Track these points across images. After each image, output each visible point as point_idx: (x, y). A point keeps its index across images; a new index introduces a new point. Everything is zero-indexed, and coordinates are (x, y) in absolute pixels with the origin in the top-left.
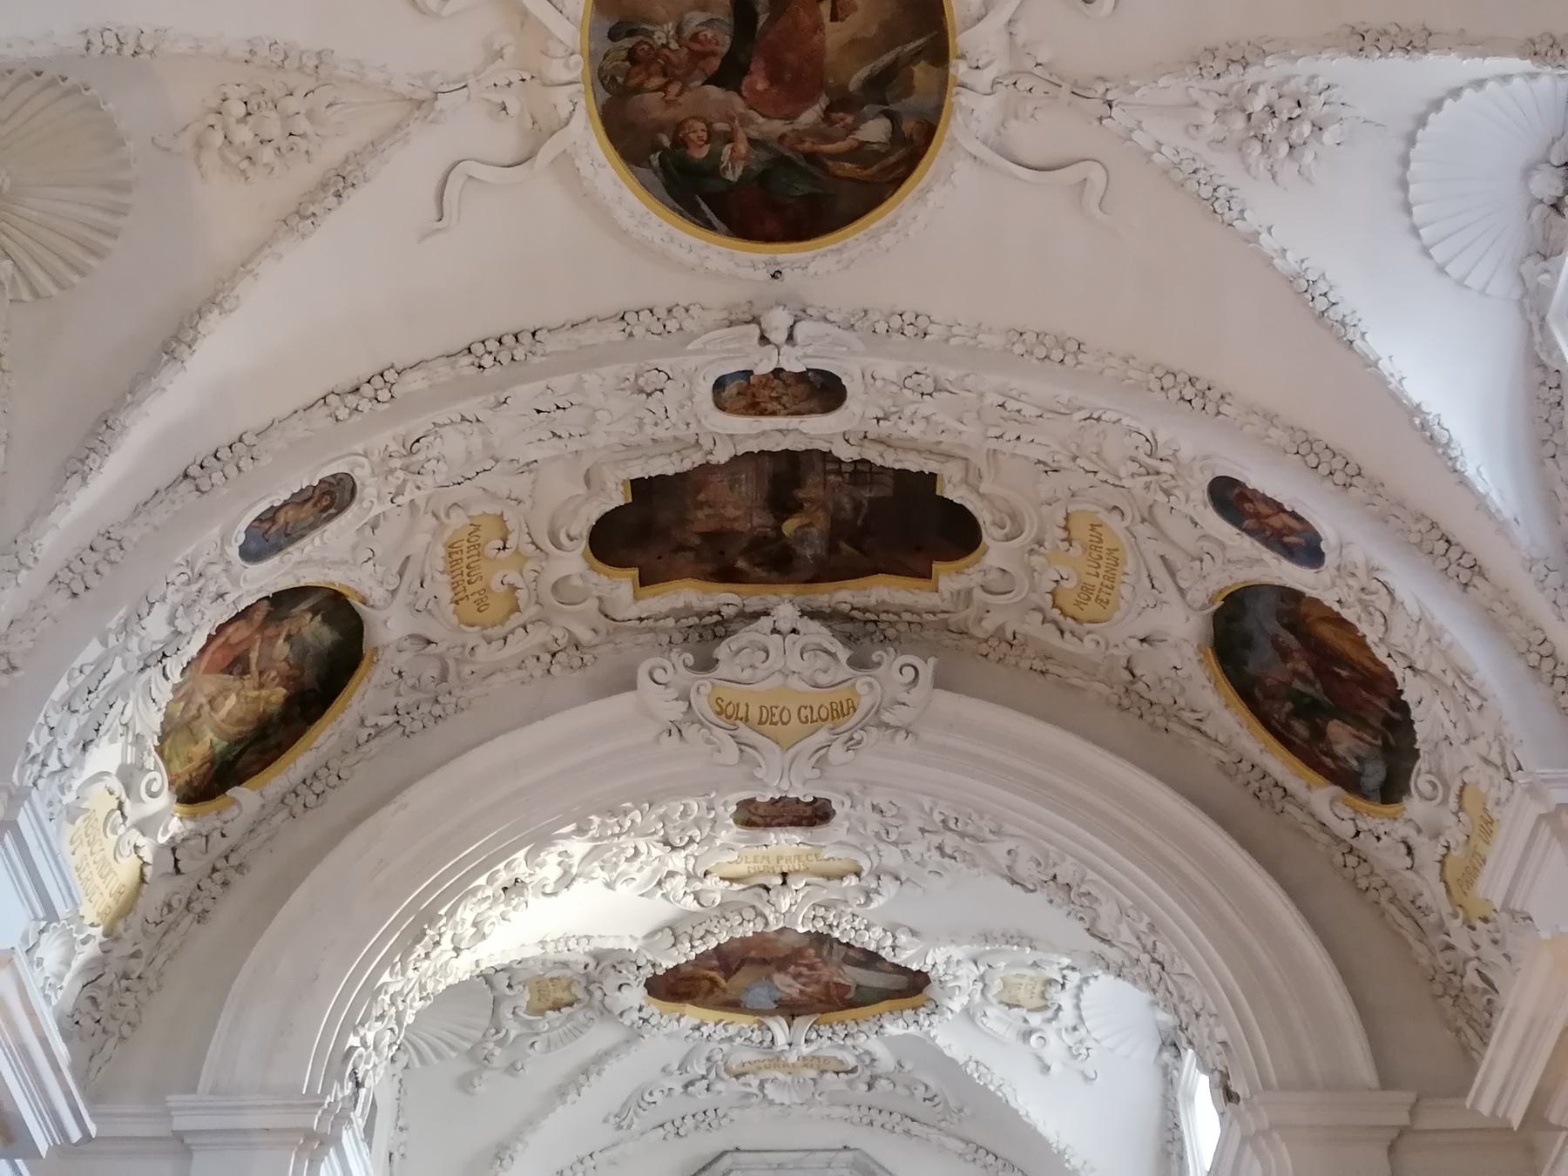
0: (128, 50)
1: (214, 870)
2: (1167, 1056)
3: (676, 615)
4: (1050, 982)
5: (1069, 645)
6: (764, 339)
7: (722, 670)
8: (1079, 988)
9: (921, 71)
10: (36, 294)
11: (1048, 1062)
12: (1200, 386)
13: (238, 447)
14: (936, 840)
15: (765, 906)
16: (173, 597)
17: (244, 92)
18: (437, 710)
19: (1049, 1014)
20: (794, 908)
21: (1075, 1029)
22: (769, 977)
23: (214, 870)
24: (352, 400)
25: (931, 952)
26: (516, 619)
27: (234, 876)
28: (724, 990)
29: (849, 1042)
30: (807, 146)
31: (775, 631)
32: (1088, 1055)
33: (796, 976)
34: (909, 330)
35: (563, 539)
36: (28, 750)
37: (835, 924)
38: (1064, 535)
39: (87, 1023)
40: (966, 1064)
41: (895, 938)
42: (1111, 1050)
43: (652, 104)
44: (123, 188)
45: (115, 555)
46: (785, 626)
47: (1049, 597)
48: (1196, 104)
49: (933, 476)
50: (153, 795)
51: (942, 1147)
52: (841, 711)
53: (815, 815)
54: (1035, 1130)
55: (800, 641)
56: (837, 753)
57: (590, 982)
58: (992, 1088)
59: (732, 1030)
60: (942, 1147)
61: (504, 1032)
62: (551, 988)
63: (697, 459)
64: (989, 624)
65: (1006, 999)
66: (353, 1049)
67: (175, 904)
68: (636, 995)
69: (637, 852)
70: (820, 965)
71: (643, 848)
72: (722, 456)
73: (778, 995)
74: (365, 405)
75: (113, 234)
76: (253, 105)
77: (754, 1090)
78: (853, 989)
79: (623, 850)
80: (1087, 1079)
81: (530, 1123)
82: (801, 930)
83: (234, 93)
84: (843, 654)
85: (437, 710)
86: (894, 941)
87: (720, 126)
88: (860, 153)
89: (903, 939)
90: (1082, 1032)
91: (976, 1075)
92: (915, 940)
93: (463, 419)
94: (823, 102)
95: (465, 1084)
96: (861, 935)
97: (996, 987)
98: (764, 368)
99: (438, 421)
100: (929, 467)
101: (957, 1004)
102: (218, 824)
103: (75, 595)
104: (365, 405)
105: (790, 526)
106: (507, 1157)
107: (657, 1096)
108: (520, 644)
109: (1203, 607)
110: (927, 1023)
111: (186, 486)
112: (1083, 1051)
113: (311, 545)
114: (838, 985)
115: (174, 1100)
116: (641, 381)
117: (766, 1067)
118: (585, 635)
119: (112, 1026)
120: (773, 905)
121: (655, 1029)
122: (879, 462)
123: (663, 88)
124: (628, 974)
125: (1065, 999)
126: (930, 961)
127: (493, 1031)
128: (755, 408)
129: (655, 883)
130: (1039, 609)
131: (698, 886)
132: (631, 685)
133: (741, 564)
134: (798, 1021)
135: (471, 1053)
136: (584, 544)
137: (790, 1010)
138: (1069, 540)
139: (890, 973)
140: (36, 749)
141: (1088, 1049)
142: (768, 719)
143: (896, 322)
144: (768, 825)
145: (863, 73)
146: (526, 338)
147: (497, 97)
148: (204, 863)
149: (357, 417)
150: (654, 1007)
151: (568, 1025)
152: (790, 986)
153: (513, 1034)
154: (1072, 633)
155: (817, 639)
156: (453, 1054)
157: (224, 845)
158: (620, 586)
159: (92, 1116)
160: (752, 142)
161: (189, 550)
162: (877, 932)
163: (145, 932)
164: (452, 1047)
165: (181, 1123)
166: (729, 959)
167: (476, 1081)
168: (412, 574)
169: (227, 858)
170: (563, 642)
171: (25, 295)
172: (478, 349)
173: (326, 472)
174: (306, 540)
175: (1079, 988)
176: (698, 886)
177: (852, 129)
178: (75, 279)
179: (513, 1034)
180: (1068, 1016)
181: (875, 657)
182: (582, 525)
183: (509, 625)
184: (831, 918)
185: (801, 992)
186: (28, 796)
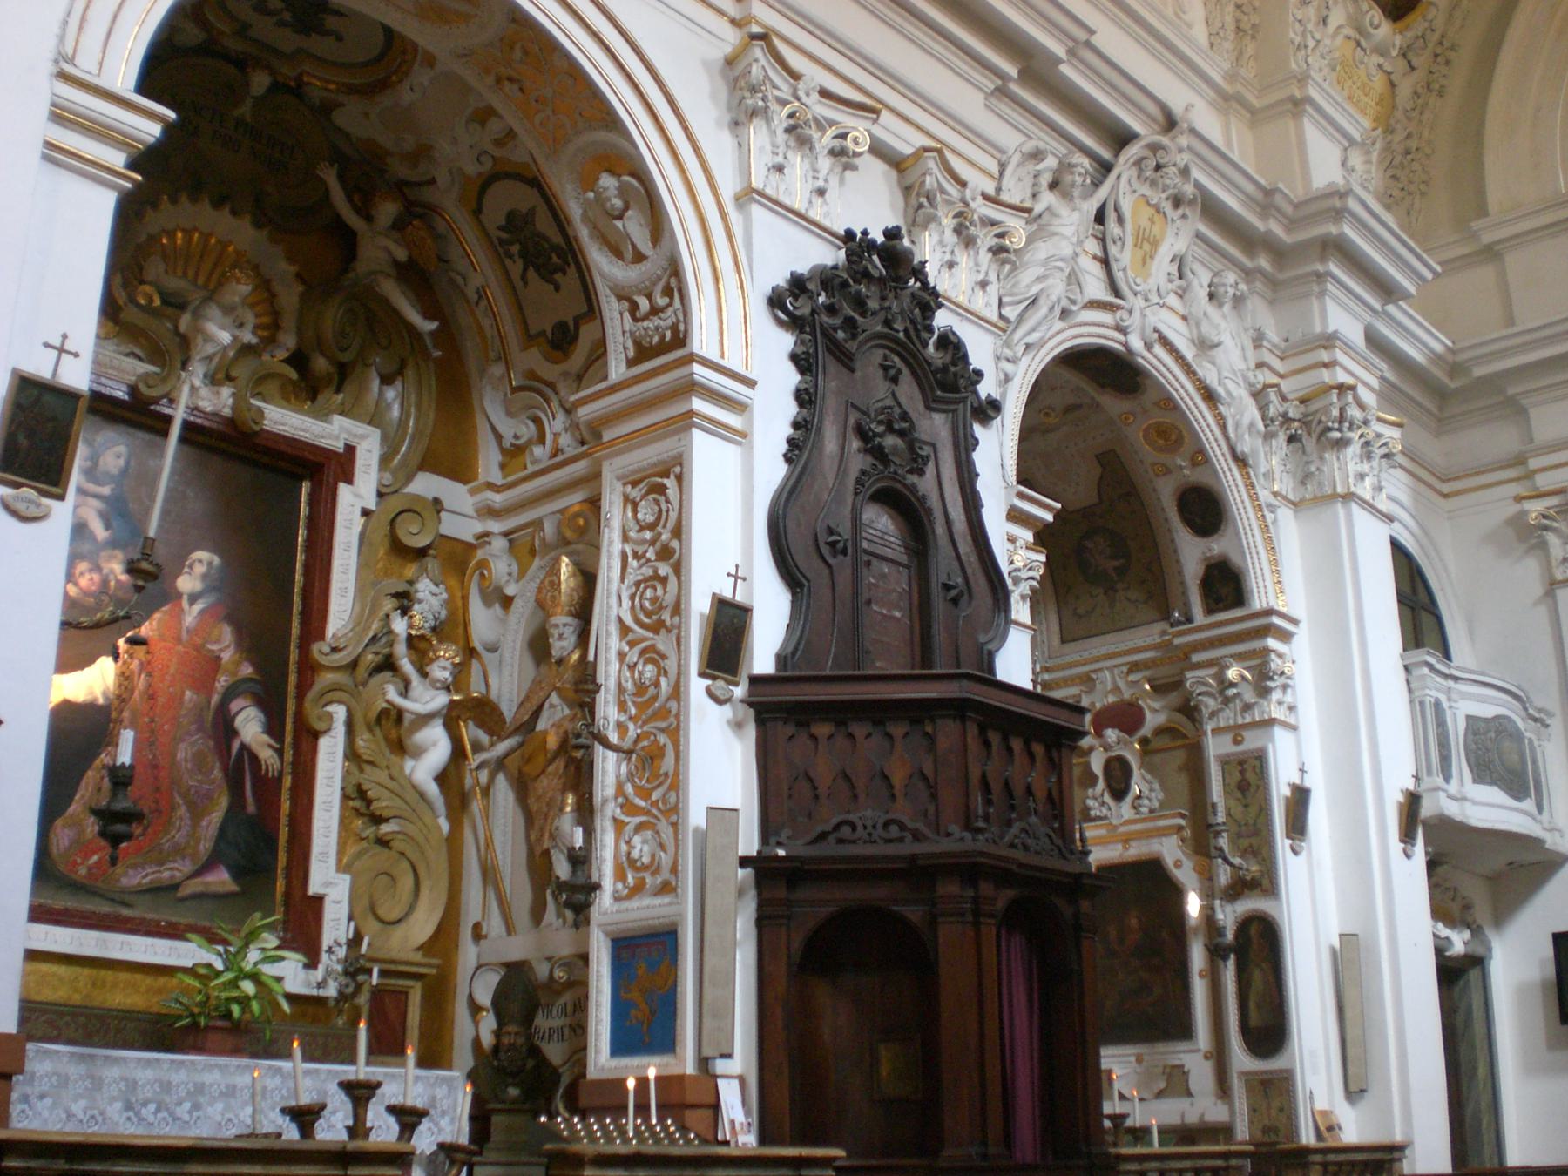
1: (1436, 56)
23: (1436, 56)
27: (1452, 55)
36: (1293, 42)
39: (1396, 193)
50: (1376, 27)
67: (1420, 90)
102: (1426, 24)
115: (1476, 225)
119: (1412, 188)
140: (1298, 40)
148: (1428, 53)
157: (1437, 36)
159: (1425, 251)
163: (1409, 119)
165: (1487, 238)
169: (1441, 43)
186: (1309, 77)
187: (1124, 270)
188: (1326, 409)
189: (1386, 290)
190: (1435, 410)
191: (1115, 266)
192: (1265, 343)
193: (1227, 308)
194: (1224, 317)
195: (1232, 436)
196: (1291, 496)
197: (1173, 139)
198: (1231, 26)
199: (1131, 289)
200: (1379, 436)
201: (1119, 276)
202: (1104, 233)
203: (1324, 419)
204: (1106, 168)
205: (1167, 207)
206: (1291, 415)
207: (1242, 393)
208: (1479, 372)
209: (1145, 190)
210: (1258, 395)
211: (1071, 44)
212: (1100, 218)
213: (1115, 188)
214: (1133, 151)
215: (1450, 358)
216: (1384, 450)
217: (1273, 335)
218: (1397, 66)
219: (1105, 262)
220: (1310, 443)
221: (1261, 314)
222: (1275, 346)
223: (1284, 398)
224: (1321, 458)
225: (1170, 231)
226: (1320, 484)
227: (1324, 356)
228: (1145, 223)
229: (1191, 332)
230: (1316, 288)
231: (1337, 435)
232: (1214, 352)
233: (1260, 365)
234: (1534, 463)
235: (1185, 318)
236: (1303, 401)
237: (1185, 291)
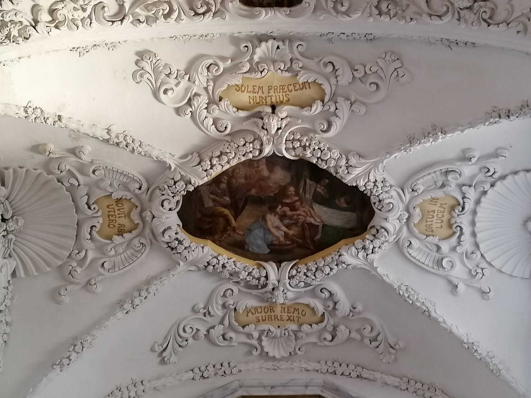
11: (455, 281)
15: (260, 131)
20: (280, 131)
22: (264, 218)
25: (372, 172)
28: (234, 229)
32: (483, 275)
37: (307, 144)
40: (399, 287)
41: (348, 160)
54: (451, 332)
58: (418, 304)
61: (83, 254)
62: (117, 212)
70: (298, 203)
73: (270, 238)
77: (255, 342)
78: (320, 229)
81: (98, 323)
86: (347, 163)
89: (353, 161)
91: (407, 295)
92: (363, 161)
96: (325, 154)
106: (79, 343)
110: (371, 247)
112: (479, 271)
114: (311, 225)
117: (264, 321)
120: (266, 130)
121: (187, 251)
127: (77, 252)
129: (186, 101)
134: (283, 265)
135: (60, 268)
139: (345, 210)
141: (482, 269)
144: (262, 5)
151: (128, 252)
152: (278, 228)
156: (48, 269)
162: (336, 154)
164: (48, 264)
167: (63, 292)
179: (91, 255)
184: (305, 140)
185: (286, 235)
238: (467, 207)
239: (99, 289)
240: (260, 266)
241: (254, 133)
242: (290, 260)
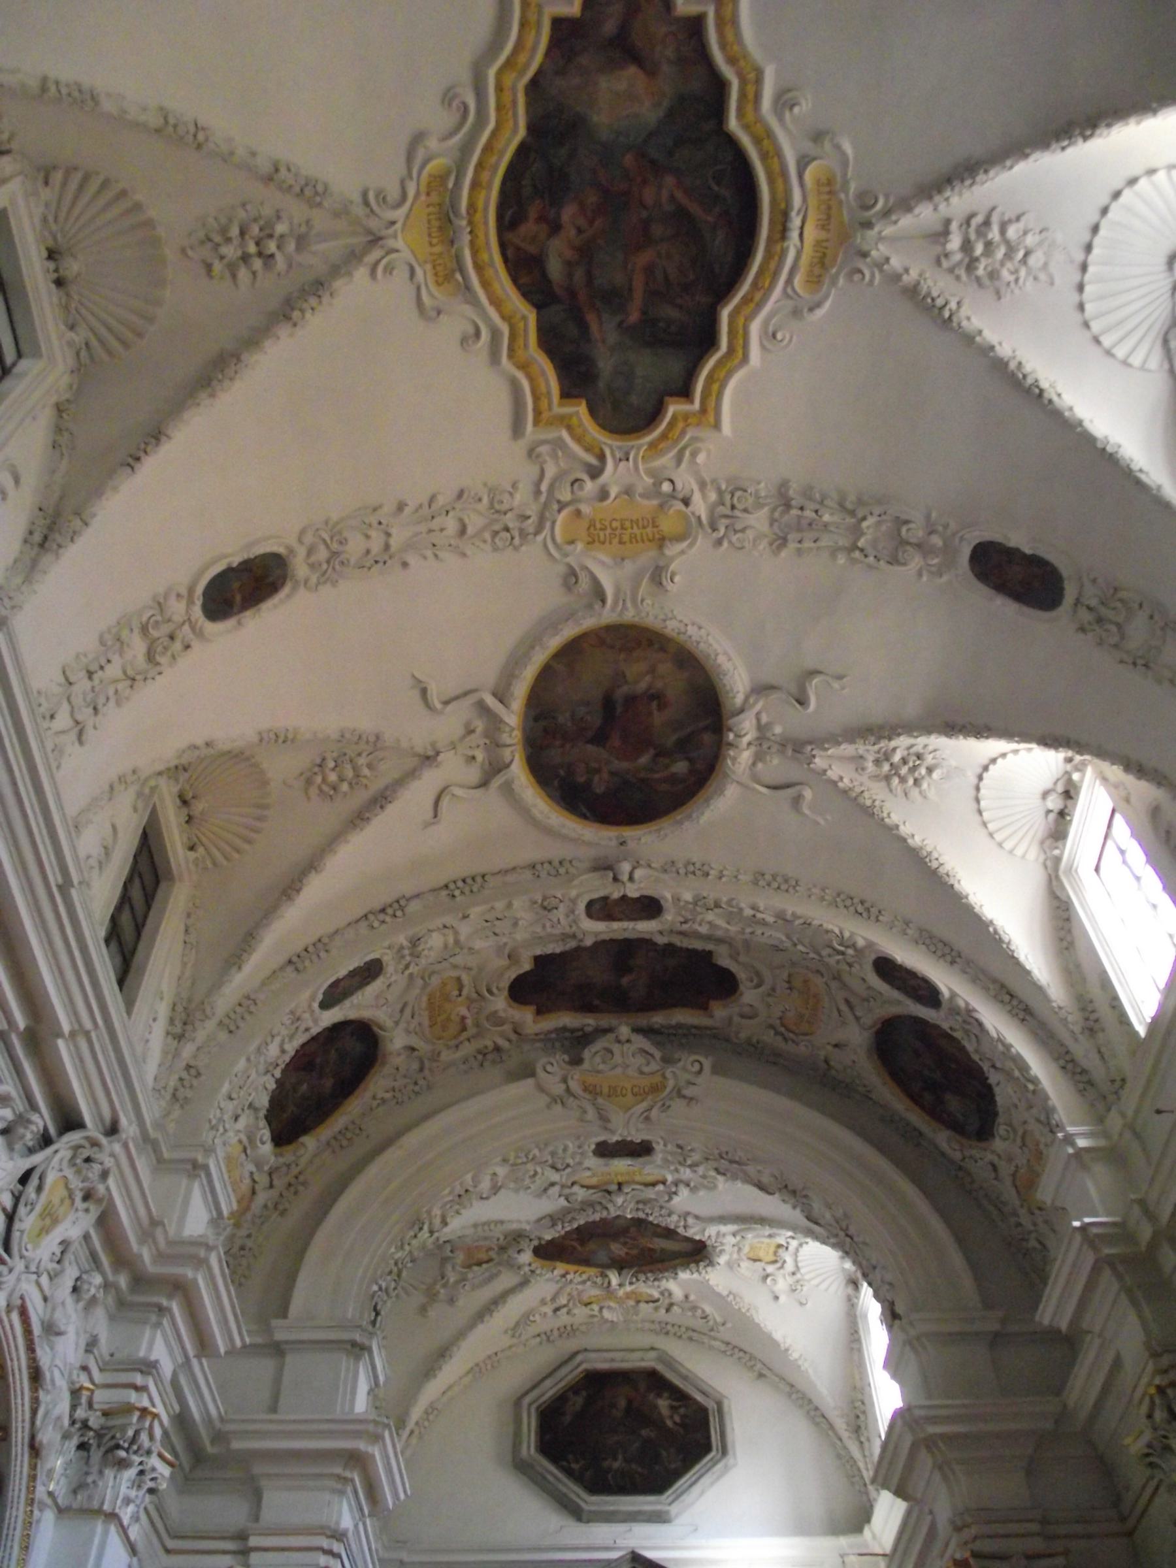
0: (281, 740)
2: (850, 1290)
3: (557, 1030)
4: (780, 1246)
5: (790, 1047)
6: (615, 879)
7: (586, 1065)
8: (797, 1250)
9: (707, 738)
10: (215, 864)
12: (866, 905)
13: (320, 945)
14: (715, 1165)
16: (284, 1032)
17: (335, 754)
18: (417, 1088)
19: (779, 1265)
21: (794, 1274)
23: (290, 1185)
24: (382, 917)
26: (465, 1035)
27: (301, 1188)
29: (656, 1283)
30: (642, 775)
31: (619, 1042)
33: (625, 1244)
34: (698, 873)
35: (495, 990)
38: (787, 985)
42: (817, 1286)
43: (555, 755)
44: (265, 807)
45: (252, 1008)
46: (623, 1038)
47: (778, 1022)
48: (861, 757)
49: (710, 953)
50: (263, 1143)
51: (711, 1348)
52: (656, 1089)
53: (642, 1150)
55: (633, 1047)
56: (654, 1113)
57: (503, 1249)
59: (584, 1277)
60: (711, 1348)
63: (572, 944)
64: (743, 1035)
65: (751, 1255)
66: (375, 1292)
67: (269, 1204)
68: (526, 1257)
69: (536, 1173)
71: (539, 1170)
72: (588, 942)
74: (388, 919)
75: (257, 831)
76: (339, 762)
77: (596, 1313)
79: (528, 1171)
80: (801, 1304)
81: (461, 1334)
82: (629, 1216)
83: (329, 756)
84: (658, 1054)
85: (417, 1088)
87: (594, 765)
88: (673, 779)
89: (690, 1220)
90: (798, 1276)
93: (445, 927)
94: (652, 751)
95: (423, 1310)
97: (746, 1250)
98: (616, 895)
99: (431, 928)
100: (710, 947)
101: (722, 1260)
102: (293, 1158)
103: (231, 1032)
104: (388, 919)
105: (625, 981)
107: (537, 1317)
108: (468, 1049)
109: (871, 1028)
111: (290, 969)
113: (358, 998)
115: (275, 1323)
116: (545, 903)
118: (501, 1042)
122: (679, 944)
123: (562, 746)
124: (524, 1244)
125: (788, 1258)
126: (707, 1234)
128: (610, 917)
130: (772, 1027)
131: (567, 1191)
132: (533, 1074)
133: (596, 1002)
134: (625, 1272)
136: (506, 993)
137: (620, 1265)
138: (790, 988)
142: (614, 1092)
143: (691, 868)
145: (674, 738)
146: (479, 879)
147: (470, 753)
149: (384, 926)
150: (537, 1264)
153: (452, 1280)
154: (793, 1041)
155: (640, 1046)
158: (525, 1016)
160: (612, 774)
161: (293, 1005)
163: (253, 1223)
165: (279, 1336)
166: (585, 1234)
168: (408, 1011)
169: (296, 1177)
170: (491, 1048)
171: (210, 865)
172: (452, 886)
173: (368, 959)
174: (354, 997)
175: (797, 1250)
176: (567, 1191)
177: (667, 767)
178: (236, 855)
179: (452, 1280)
180: (790, 1266)
181: (676, 1056)
182: (505, 984)
183: (461, 1038)
187: (22, 1232)
188: (123, 1428)
189: (204, 1344)
190: (187, 1467)
191: (17, 1225)
192: (96, 1351)
193: (81, 1304)
194: (76, 1310)
195: (38, 1423)
196: (60, 1501)
197: (110, 1143)
198: (170, 1090)
199: (20, 1251)
200: (154, 1469)
201: (16, 1235)
202: (21, 1193)
203: (118, 1435)
204: (46, 1141)
205: (78, 1196)
206: (90, 1423)
207: (62, 1383)
208: (236, 1445)
209: (69, 1173)
210: (75, 1393)
211: (76, 1027)
212: (24, 1179)
213: (48, 1160)
214: (74, 1137)
215: (218, 1424)
216: (150, 1484)
217: (104, 1347)
218: (263, 1180)
219: (11, 1218)
220: (96, 1455)
221: (100, 1323)
222: (101, 1356)
223: (90, 1405)
224: (101, 1473)
225: (71, 1217)
226: (90, 1498)
227: (139, 1379)
228: (56, 1201)
229: (45, 1312)
230: (154, 1318)
231: (123, 1454)
232: (53, 1338)
233: (85, 1368)
234: (253, 1541)
235: (45, 1299)
236: (105, 1414)
237: (56, 1275)
238: (790, 1248)
239: (461, 1303)
240: (603, 1275)
241: (600, 1203)
242: (631, 1267)
